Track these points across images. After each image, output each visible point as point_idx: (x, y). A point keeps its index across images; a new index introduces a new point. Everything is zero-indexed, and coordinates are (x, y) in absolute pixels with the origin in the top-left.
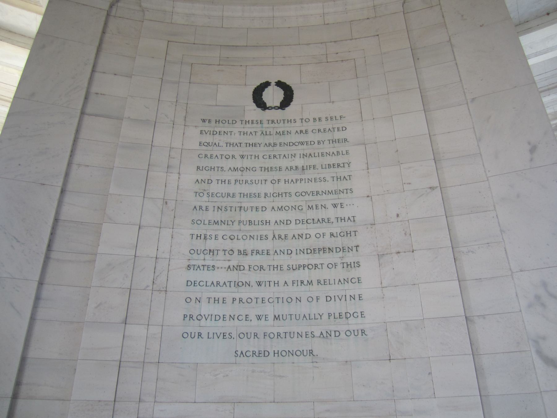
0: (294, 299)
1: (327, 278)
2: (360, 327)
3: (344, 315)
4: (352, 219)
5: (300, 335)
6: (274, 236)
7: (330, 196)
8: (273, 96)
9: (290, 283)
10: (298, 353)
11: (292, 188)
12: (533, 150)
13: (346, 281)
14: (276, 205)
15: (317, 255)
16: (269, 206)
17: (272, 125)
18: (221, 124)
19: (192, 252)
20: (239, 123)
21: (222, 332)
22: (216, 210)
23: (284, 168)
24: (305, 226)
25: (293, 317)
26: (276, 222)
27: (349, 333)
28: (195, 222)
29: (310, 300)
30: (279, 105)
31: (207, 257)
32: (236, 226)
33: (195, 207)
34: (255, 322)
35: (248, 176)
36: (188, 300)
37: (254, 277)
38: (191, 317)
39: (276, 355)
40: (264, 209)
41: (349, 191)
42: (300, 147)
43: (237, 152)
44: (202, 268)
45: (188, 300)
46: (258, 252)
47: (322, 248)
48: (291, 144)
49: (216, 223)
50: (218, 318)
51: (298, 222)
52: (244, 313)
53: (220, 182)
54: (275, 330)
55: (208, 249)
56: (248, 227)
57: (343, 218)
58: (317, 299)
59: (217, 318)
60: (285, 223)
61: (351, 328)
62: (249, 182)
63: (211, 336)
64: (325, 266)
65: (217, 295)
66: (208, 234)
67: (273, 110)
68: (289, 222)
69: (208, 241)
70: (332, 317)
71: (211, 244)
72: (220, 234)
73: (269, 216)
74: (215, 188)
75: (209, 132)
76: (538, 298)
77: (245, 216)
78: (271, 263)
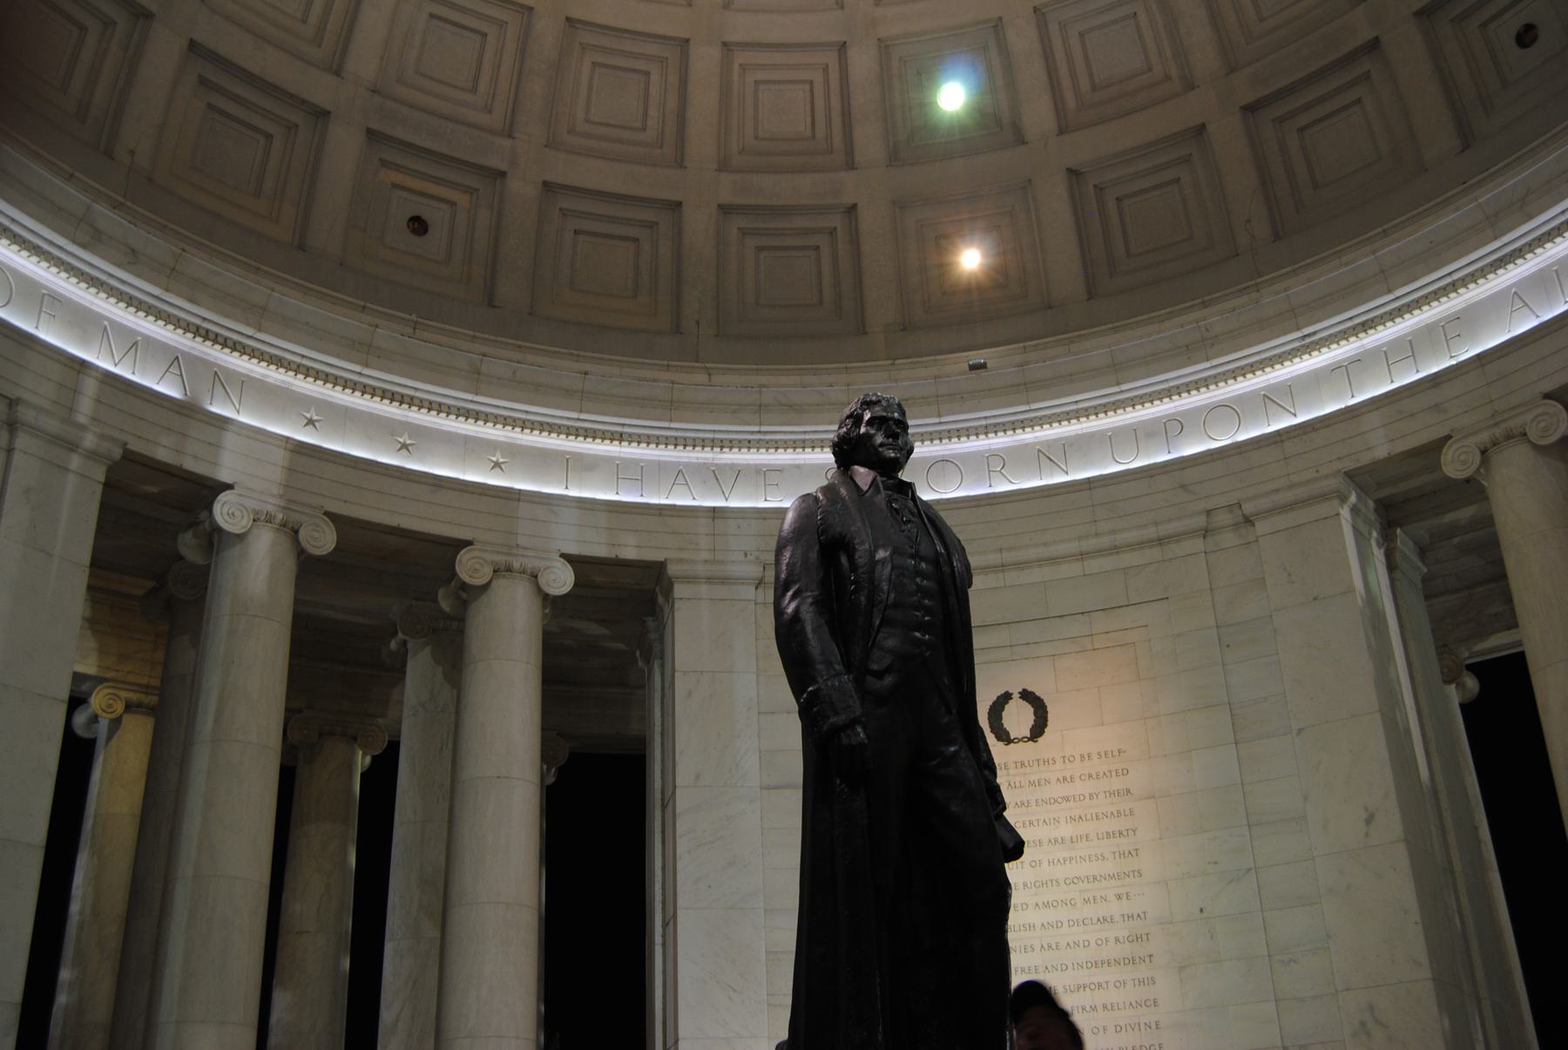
7: (1113, 882)
12: (1369, 820)
23: (1045, 842)
42: (1064, 805)
64: (1111, 985)
76: (1363, 1024)
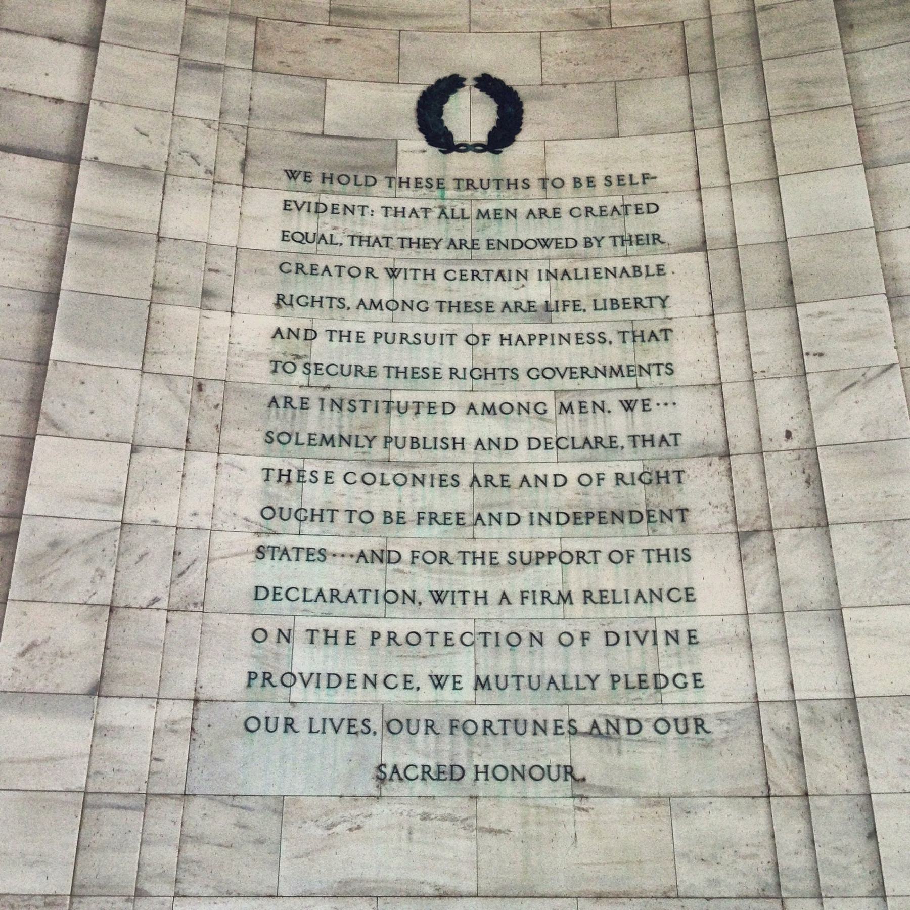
0: (525, 636)
1: (609, 586)
2: (693, 711)
3: (650, 682)
4: (671, 440)
5: (539, 727)
6: (475, 478)
7: (616, 382)
8: (469, 116)
9: (515, 599)
10: (537, 773)
11: (520, 358)
13: (656, 595)
14: (479, 399)
15: (583, 529)
16: (462, 400)
17: (469, 192)
18: (337, 186)
19: (268, 513)
20: (382, 185)
21: (346, 717)
22: (327, 408)
23: (498, 306)
24: (553, 454)
25: (524, 682)
26: (480, 442)
27: (663, 725)
28: (274, 436)
29: (565, 641)
30: (483, 139)
31: (306, 527)
32: (378, 451)
33: (274, 400)
34: (428, 693)
35: (410, 323)
36: (260, 636)
37: (422, 581)
38: (267, 678)
39: (482, 776)
40: (449, 409)
41: (663, 369)
42: (539, 252)
43: (378, 258)
44: (293, 555)
45: (258, 636)
46: (433, 517)
47: (595, 511)
48: (517, 244)
49: (327, 441)
50: (334, 681)
51: (534, 444)
52: (398, 668)
53: (336, 337)
54: (479, 715)
55: (309, 508)
56: (408, 455)
57: (647, 437)
58: (585, 637)
59: (333, 681)
60: (503, 446)
61: (670, 712)
62: (411, 339)
63: (317, 726)
64: (602, 558)
65: (333, 624)
66: (309, 468)
67: (470, 153)
68: (512, 444)
69: (308, 487)
70: (621, 686)
71: (315, 495)
72: (339, 469)
73: (459, 425)
74: (322, 351)
75: (306, 206)
77: (398, 426)
78: (468, 546)
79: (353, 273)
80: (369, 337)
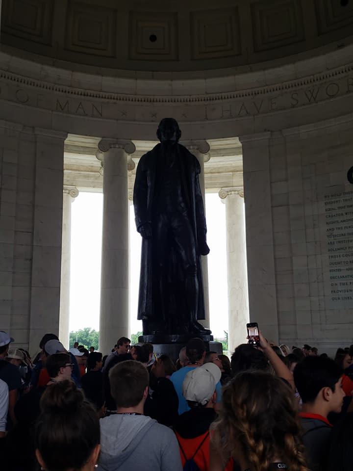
38: (334, 292)
49: (339, 249)
59: (345, 291)
71: (338, 260)
74: (336, 232)
79: (339, 215)
80: (343, 228)
